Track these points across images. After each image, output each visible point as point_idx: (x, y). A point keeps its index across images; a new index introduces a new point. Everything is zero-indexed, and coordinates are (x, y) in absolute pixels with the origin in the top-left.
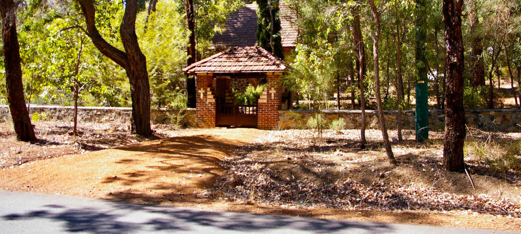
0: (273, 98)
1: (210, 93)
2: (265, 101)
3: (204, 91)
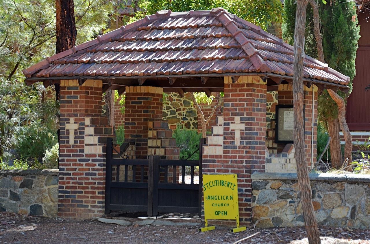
0: (237, 143)
1: (89, 130)
2: (220, 151)
3: (76, 126)
